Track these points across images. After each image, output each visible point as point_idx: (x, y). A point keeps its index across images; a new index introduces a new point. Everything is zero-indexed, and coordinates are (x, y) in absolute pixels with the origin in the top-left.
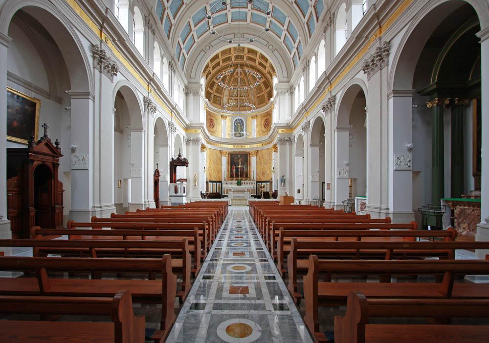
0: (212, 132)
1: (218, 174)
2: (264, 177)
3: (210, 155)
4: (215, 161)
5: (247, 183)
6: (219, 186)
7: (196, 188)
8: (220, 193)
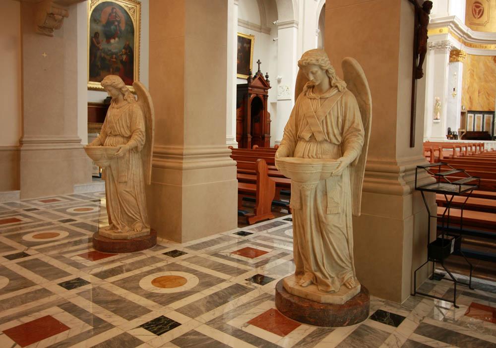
0: (479, 25)
1: (488, 99)
3: (473, 65)
6: (489, 119)
7: (437, 123)
8: (491, 134)
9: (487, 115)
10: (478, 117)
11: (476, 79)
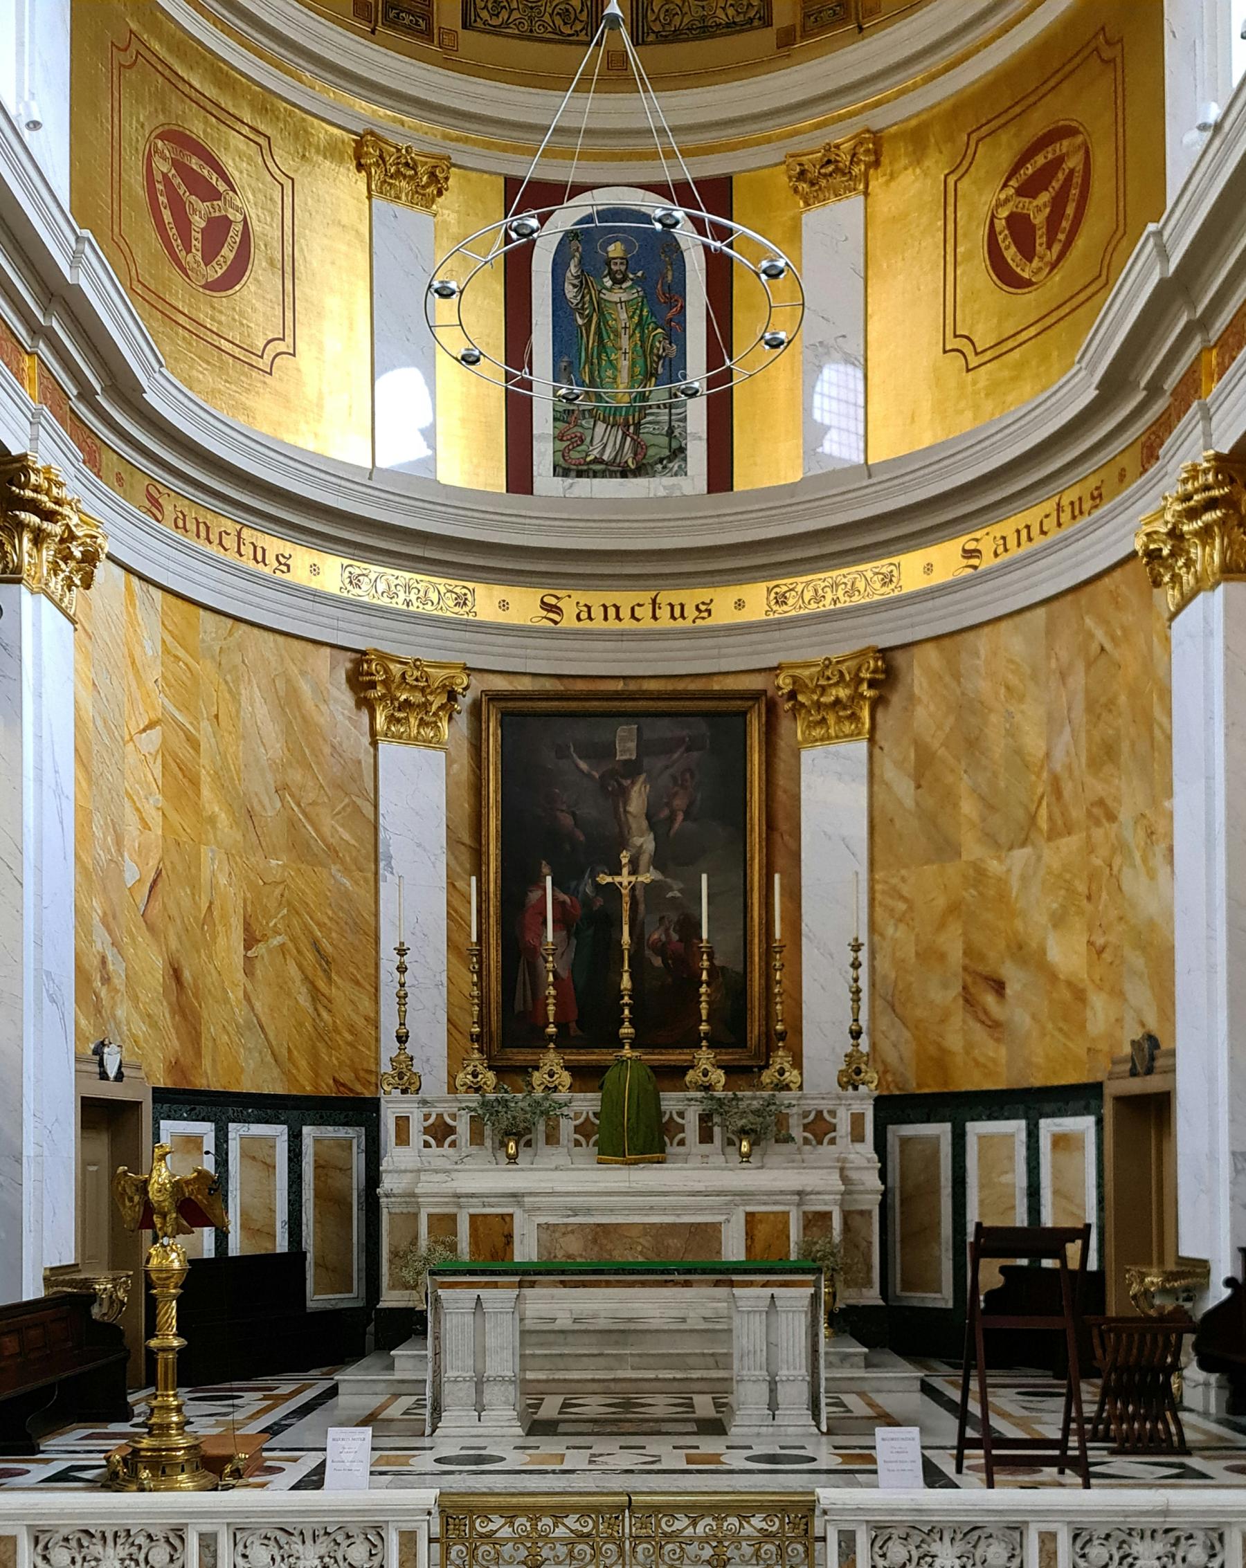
1: (316, 994)
2: (994, 1026)
4: (270, 808)
9: (329, 1132)
11: (223, 819)
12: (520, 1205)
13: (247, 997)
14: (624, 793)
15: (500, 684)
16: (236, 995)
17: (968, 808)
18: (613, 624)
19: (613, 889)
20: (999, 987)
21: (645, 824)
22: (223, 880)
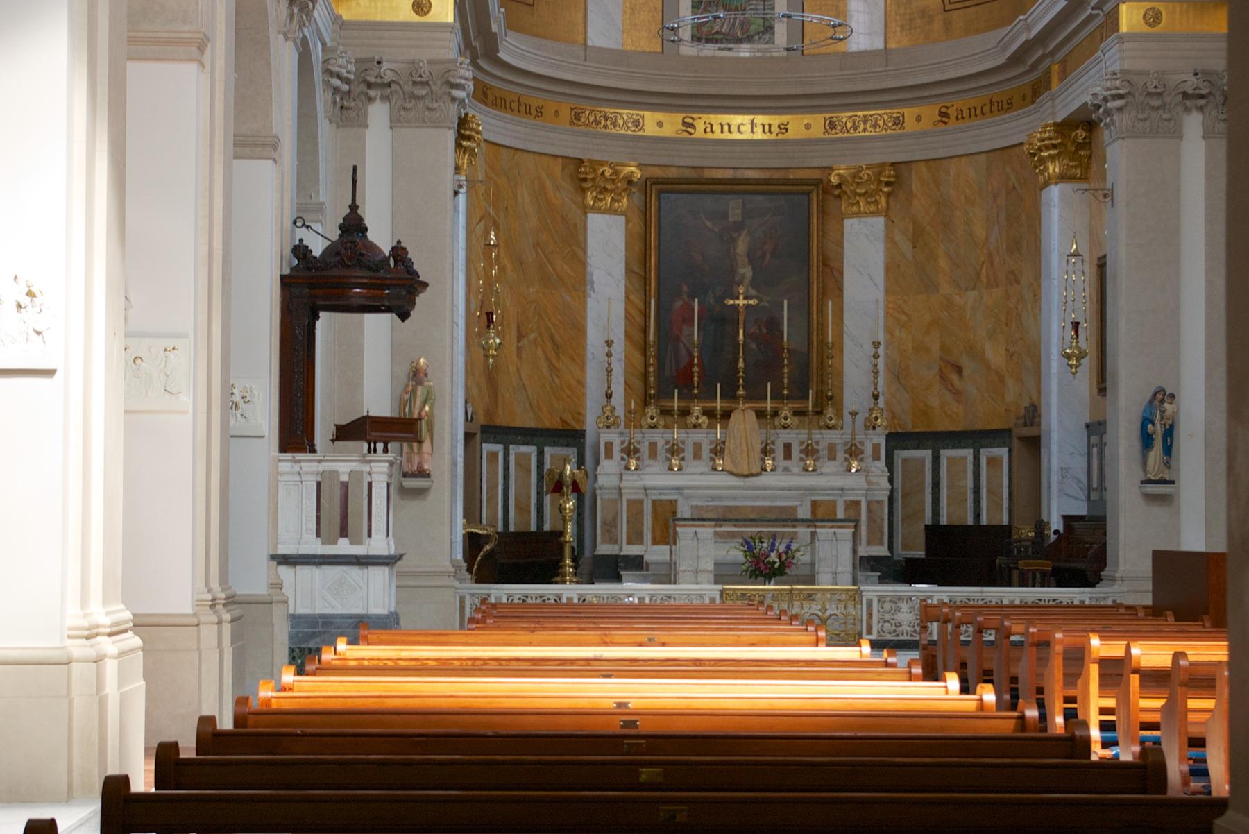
1: (551, 366)
5: (809, 451)
10: (518, 455)
12: (681, 494)
13: (518, 370)
14: (733, 241)
15: (658, 173)
16: (512, 369)
17: (943, 263)
18: (727, 136)
19: (735, 307)
20: (959, 370)
21: (746, 260)
22: (508, 303)
